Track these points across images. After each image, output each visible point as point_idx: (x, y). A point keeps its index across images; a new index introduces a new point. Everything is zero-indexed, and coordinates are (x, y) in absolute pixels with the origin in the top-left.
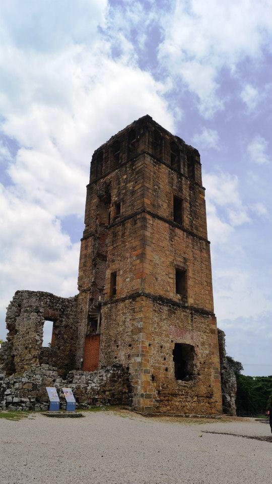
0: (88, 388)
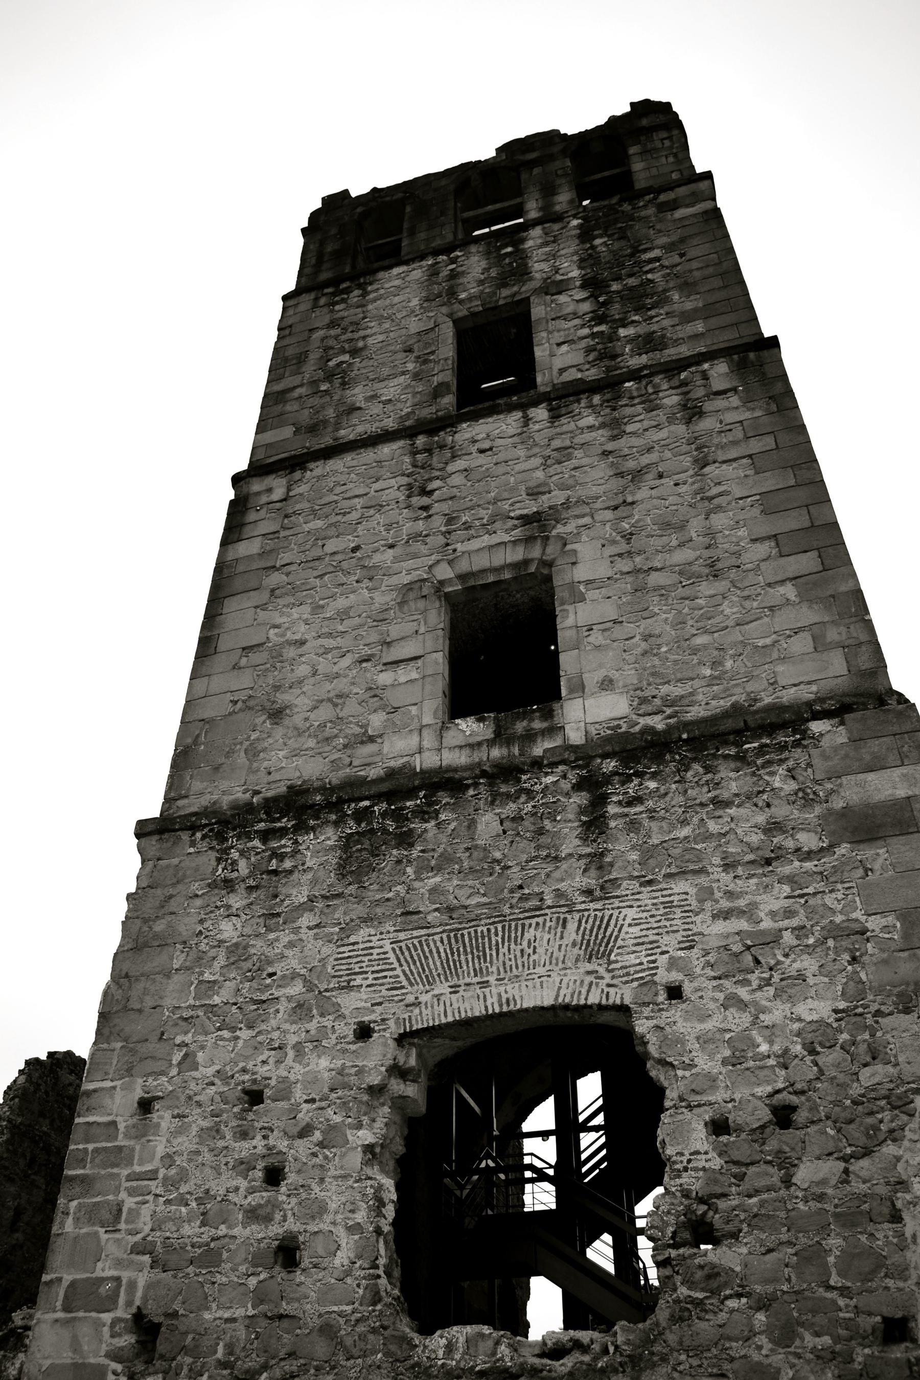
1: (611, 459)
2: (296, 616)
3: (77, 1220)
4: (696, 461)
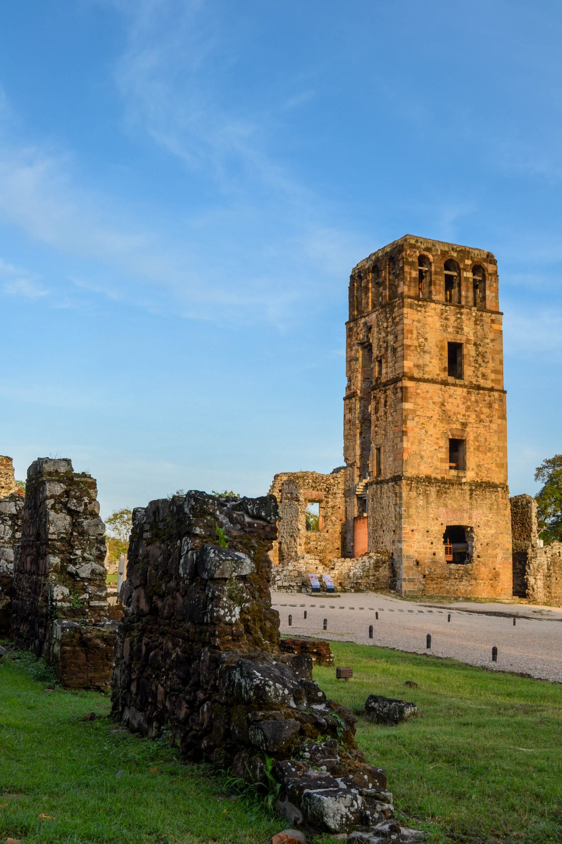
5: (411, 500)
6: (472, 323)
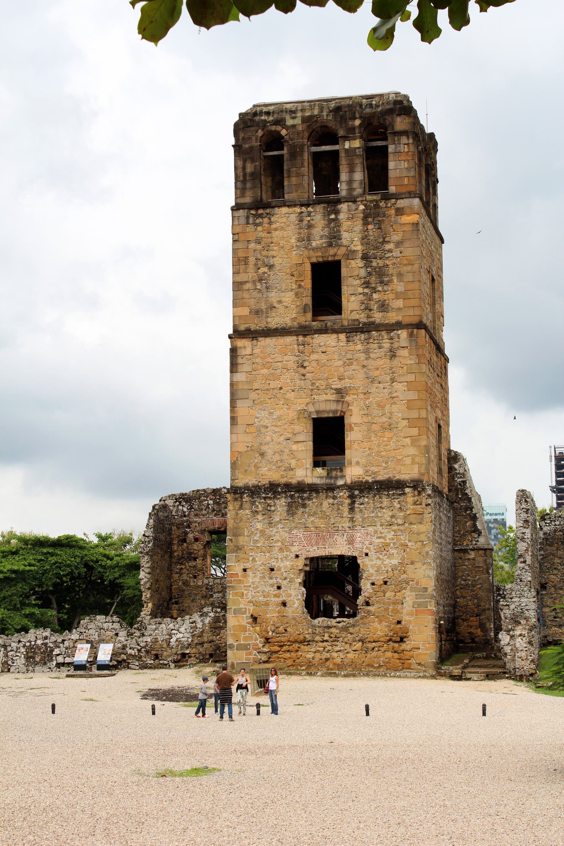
0: (171, 640)
1: (365, 370)
2: (263, 415)
3: (233, 596)
4: (391, 379)
5: (241, 524)
6: (360, 222)
